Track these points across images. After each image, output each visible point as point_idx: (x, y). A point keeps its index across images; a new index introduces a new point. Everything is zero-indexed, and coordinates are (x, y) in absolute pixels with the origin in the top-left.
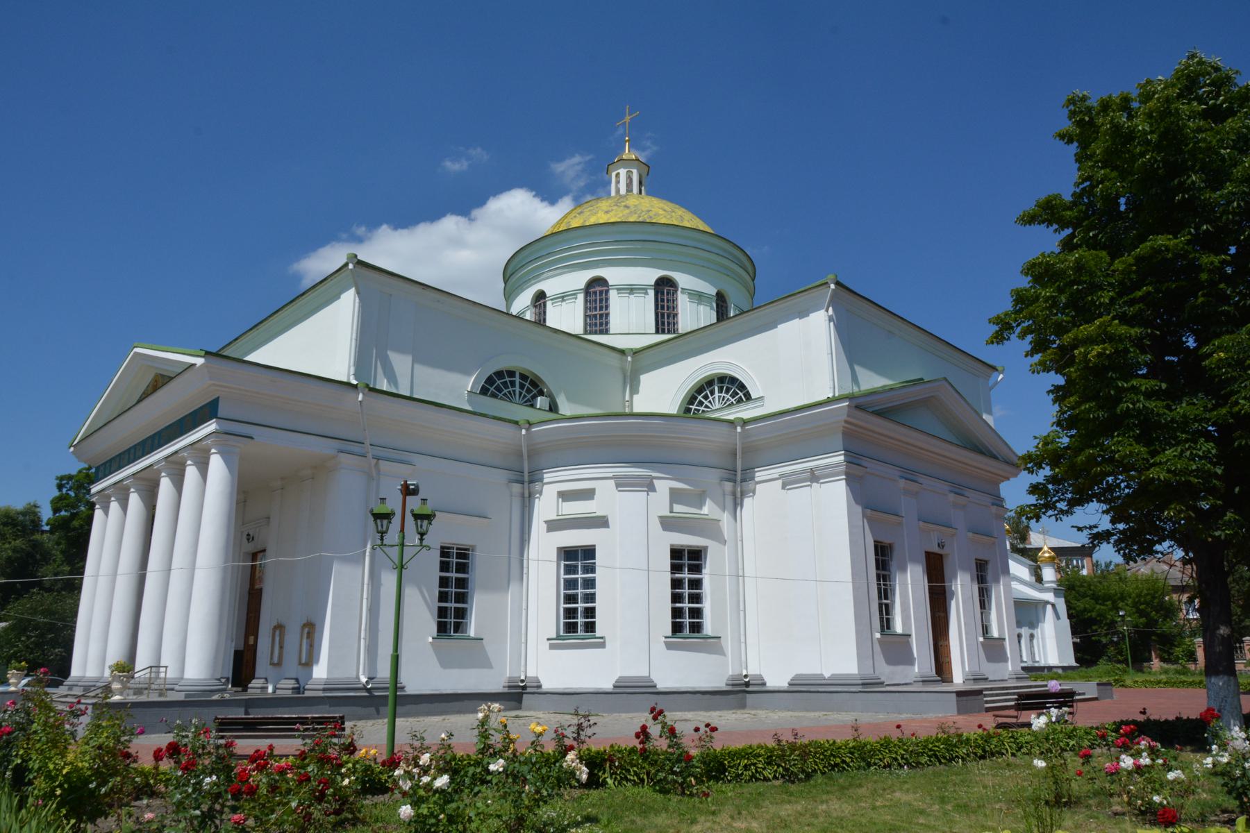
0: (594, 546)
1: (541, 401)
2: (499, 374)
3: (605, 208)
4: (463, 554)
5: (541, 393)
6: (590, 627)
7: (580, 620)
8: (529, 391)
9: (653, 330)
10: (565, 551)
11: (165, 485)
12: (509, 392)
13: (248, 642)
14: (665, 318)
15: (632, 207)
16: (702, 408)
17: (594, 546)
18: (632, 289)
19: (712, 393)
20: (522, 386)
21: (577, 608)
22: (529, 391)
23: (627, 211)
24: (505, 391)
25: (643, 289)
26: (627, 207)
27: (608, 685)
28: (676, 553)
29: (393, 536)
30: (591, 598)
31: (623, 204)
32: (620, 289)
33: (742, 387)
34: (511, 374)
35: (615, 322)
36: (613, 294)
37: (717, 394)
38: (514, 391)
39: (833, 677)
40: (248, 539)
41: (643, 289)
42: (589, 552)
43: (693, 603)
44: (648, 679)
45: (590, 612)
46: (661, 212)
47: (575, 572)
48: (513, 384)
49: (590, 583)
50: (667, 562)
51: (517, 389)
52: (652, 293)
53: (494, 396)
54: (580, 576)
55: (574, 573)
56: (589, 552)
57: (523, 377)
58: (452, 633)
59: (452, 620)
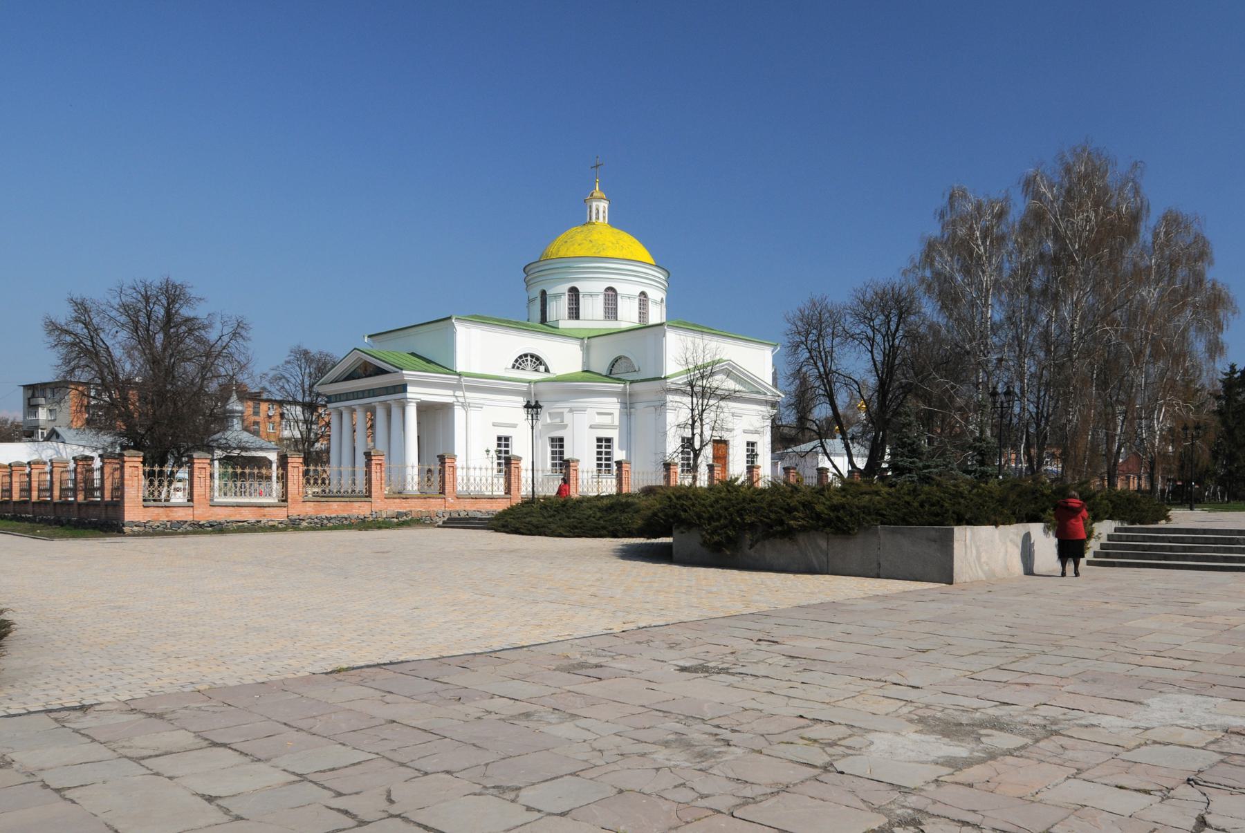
1: (542, 368)
2: (520, 357)
3: (579, 242)
4: (507, 439)
5: (541, 363)
9: (602, 318)
11: (381, 414)
14: (611, 311)
20: (531, 361)
22: (535, 363)
23: (591, 245)
26: (590, 241)
28: (599, 440)
29: (490, 456)
34: (526, 355)
35: (582, 312)
36: (581, 296)
42: (561, 440)
46: (610, 245)
48: (527, 360)
50: (595, 443)
51: (529, 362)
52: (601, 298)
53: (518, 368)
57: (532, 356)
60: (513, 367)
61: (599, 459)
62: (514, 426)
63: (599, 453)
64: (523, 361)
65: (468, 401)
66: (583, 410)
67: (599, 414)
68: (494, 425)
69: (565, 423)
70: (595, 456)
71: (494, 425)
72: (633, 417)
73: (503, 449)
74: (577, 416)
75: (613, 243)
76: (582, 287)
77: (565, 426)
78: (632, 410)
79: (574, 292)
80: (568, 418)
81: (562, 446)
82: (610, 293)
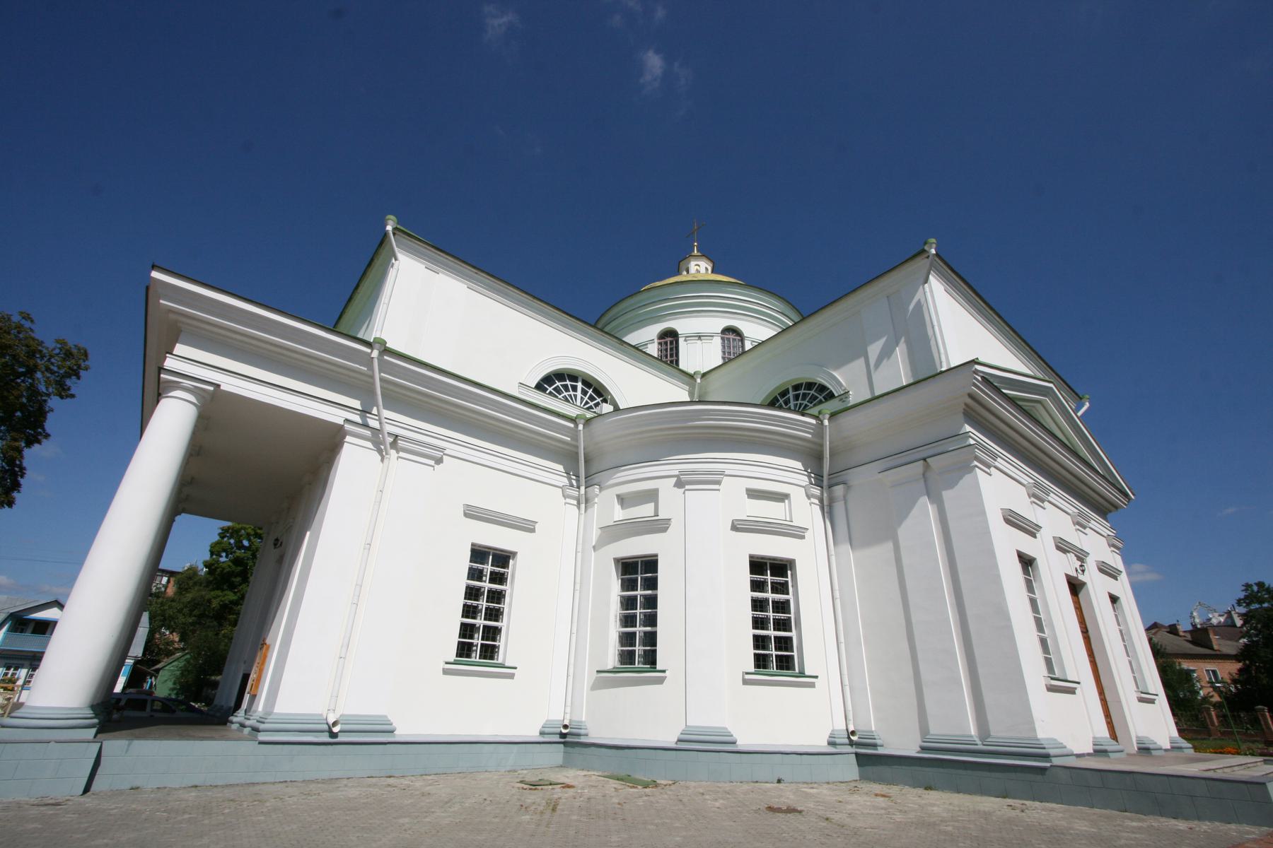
0: (656, 556)
4: (503, 558)
5: (605, 401)
6: (650, 658)
7: (639, 649)
8: (592, 398)
10: (622, 563)
12: (570, 396)
17: (656, 556)
18: (700, 336)
20: (584, 393)
21: (634, 634)
22: (592, 398)
24: (565, 394)
25: (711, 336)
32: (687, 338)
33: (822, 388)
34: (574, 378)
36: (681, 341)
38: (575, 396)
40: (275, 545)
41: (711, 336)
42: (650, 564)
43: (779, 630)
47: (635, 589)
48: (575, 389)
50: (746, 577)
51: (579, 393)
52: (717, 341)
54: (640, 592)
55: (633, 590)
56: (650, 564)
58: (478, 660)
59: (478, 640)
60: (539, 387)
61: (759, 623)
62: (527, 526)
63: (758, 605)
64: (566, 387)
65: (389, 428)
66: (713, 481)
67: (753, 494)
68: (472, 513)
69: (663, 515)
70: (748, 614)
71: (472, 513)
73: (486, 585)
74: (697, 498)
76: (682, 325)
77: (658, 526)
78: (839, 490)
79: (669, 338)
80: (671, 501)
81: (652, 584)
82: (732, 336)
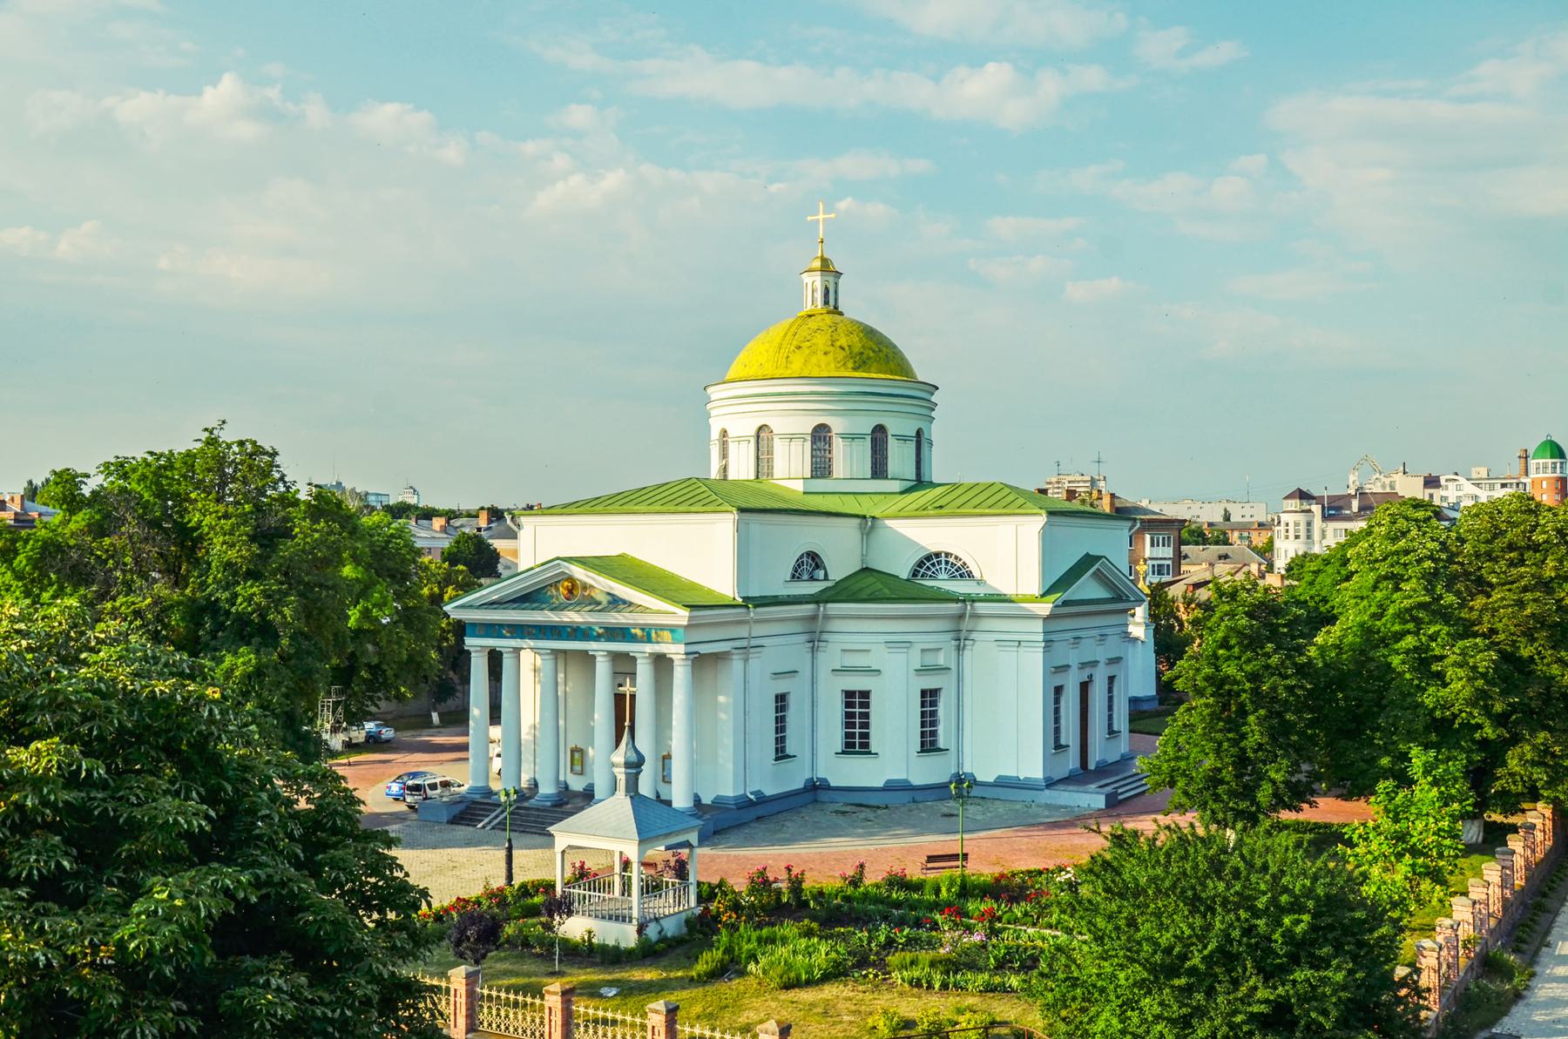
1: (821, 574)
6: (865, 745)
13: (633, 763)
14: (879, 470)
15: (847, 348)
16: (930, 573)
19: (939, 563)
25: (861, 437)
27: (881, 784)
28: (924, 693)
30: (866, 725)
31: (838, 344)
37: (943, 566)
39: (1026, 779)
41: (861, 437)
42: (865, 694)
44: (906, 781)
45: (866, 736)
46: (872, 354)
49: (867, 715)
56: (865, 694)
60: (793, 576)
72: (967, 653)
75: (874, 351)
